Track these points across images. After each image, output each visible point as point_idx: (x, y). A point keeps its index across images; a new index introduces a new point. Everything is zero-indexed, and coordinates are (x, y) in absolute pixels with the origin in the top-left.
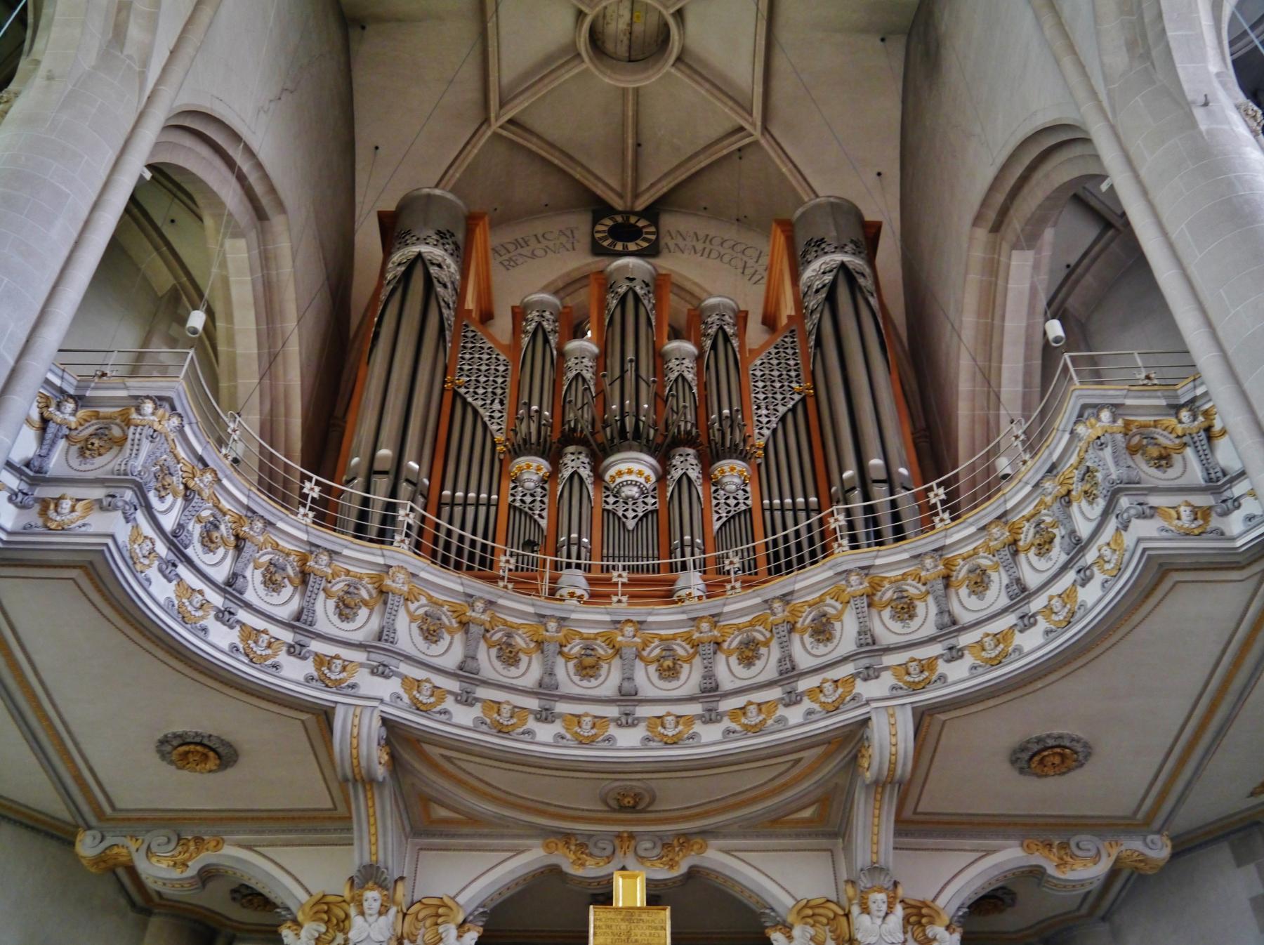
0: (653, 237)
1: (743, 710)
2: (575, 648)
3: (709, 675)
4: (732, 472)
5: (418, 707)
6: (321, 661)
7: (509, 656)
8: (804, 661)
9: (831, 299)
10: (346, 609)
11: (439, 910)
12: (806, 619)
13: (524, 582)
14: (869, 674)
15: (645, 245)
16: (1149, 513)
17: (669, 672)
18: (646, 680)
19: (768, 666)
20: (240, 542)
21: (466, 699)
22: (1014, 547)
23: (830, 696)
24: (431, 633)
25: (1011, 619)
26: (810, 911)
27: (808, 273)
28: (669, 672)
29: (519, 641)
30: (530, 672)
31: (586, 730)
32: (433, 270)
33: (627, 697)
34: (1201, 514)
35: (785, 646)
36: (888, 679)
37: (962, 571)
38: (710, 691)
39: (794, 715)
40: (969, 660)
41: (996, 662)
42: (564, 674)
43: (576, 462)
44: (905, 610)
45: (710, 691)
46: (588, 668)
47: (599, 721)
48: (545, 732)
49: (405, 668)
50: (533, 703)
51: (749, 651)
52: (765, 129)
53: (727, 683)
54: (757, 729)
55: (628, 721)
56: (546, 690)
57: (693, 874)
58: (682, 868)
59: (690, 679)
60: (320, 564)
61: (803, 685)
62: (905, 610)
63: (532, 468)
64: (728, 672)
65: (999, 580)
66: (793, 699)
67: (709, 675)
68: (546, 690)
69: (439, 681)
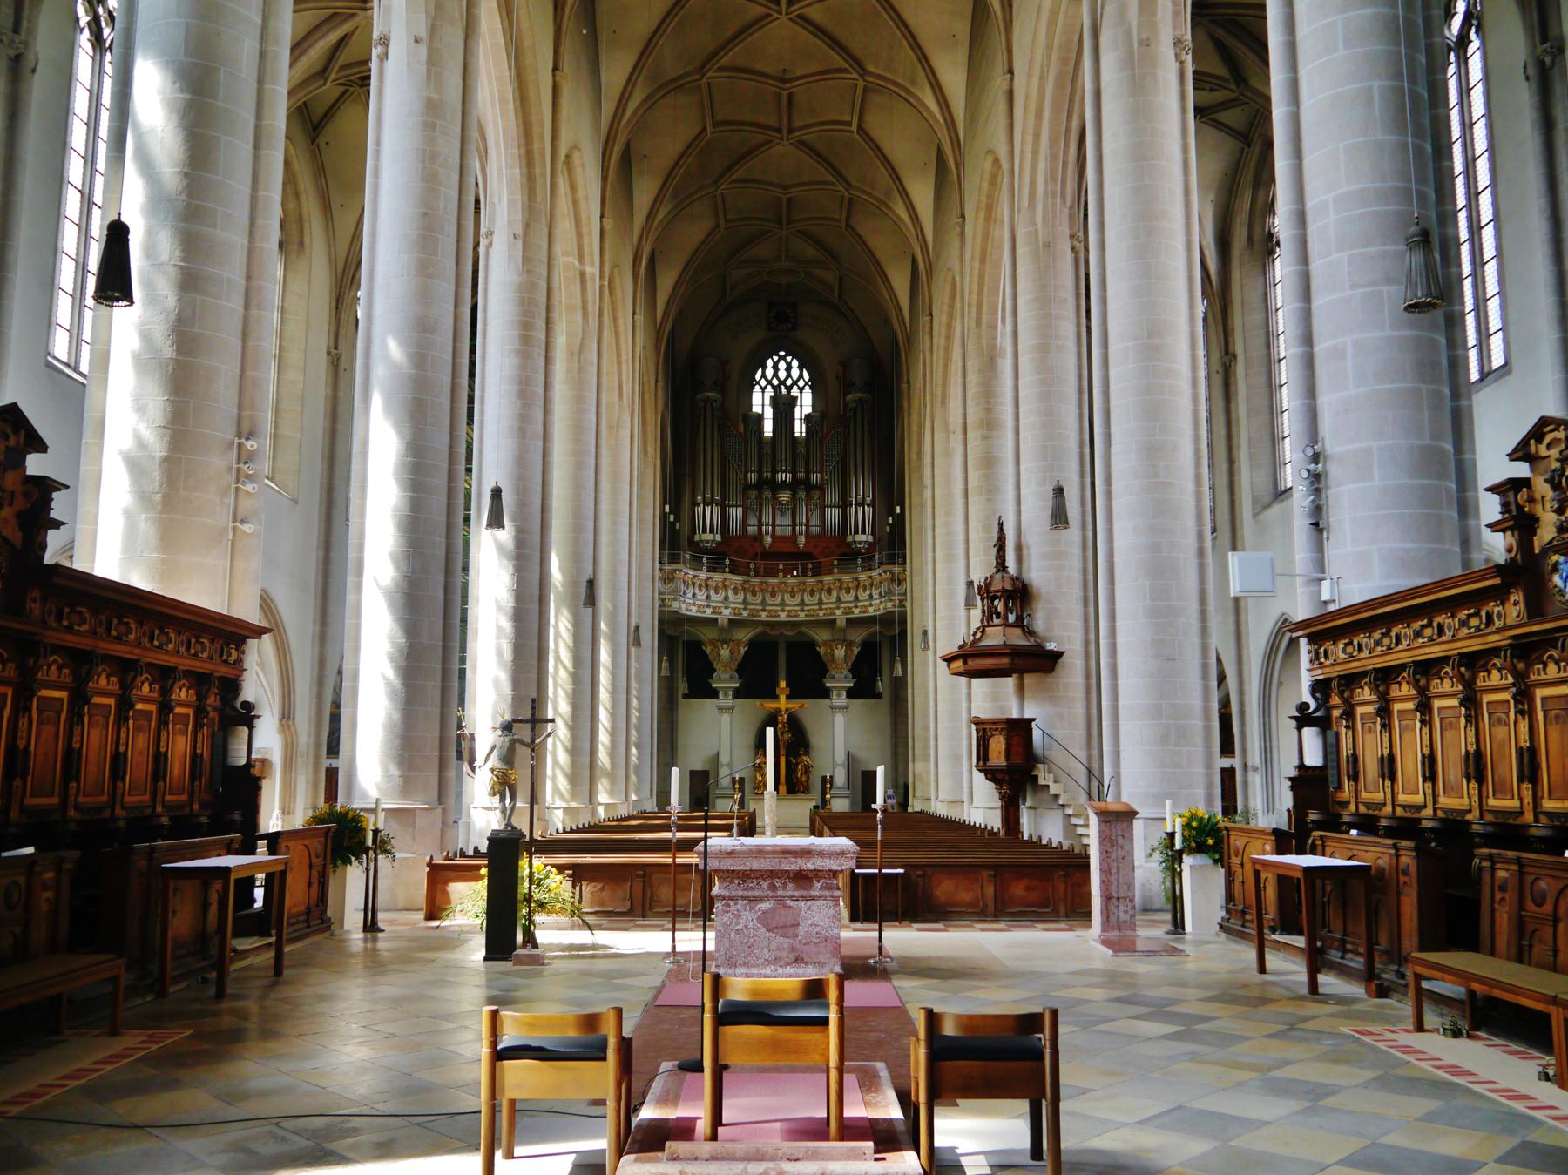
0: (793, 320)
1: (809, 611)
2: (770, 589)
3: (802, 600)
4: (816, 494)
5: (735, 614)
6: (714, 608)
7: (754, 593)
8: (825, 600)
9: (855, 414)
10: (717, 592)
11: (738, 643)
12: (826, 587)
13: (757, 575)
14: (838, 608)
15: (790, 325)
16: (890, 600)
17: (793, 597)
18: (787, 597)
19: (816, 599)
20: (694, 584)
21: (745, 609)
22: (872, 585)
23: (829, 611)
24: (736, 593)
25: (867, 603)
26: (826, 643)
27: (849, 397)
28: (793, 596)
29: (757, 589)
30: (759, 598)
31: (773, 614)
32: (714, 404)
33: (783, 604)
34: (901, 601)
35: (820, 595)
36: (842, 610)
37: (862, 584)
38: (802, 603)
39: (821, 613)
40: (859, 610)
41: (865, 612)
42: (767, 597)
43: (767, 493)
44: (848, 591)
45: (802, 603)
46: (773, 595)
47: (776, 611)
48: (764, 615)
49: (732, 606)
50: (761, 608)
51: (812, 593)
52: (840, 296)
53: (807, 602)
54: (813, 616)
55: (783, 610)
56: (763, 603)
57: (799, 632)
58: (796, 632)
59: (797, 600)
60: (710, 582)
61: (824, 607)
62: (848, 591)
63: (753, 494)
64: (807, 598)
65: (868, 592)
66: (821, 609)
67: (802, 600)
68: (763, 603)
69: (739, 606)
